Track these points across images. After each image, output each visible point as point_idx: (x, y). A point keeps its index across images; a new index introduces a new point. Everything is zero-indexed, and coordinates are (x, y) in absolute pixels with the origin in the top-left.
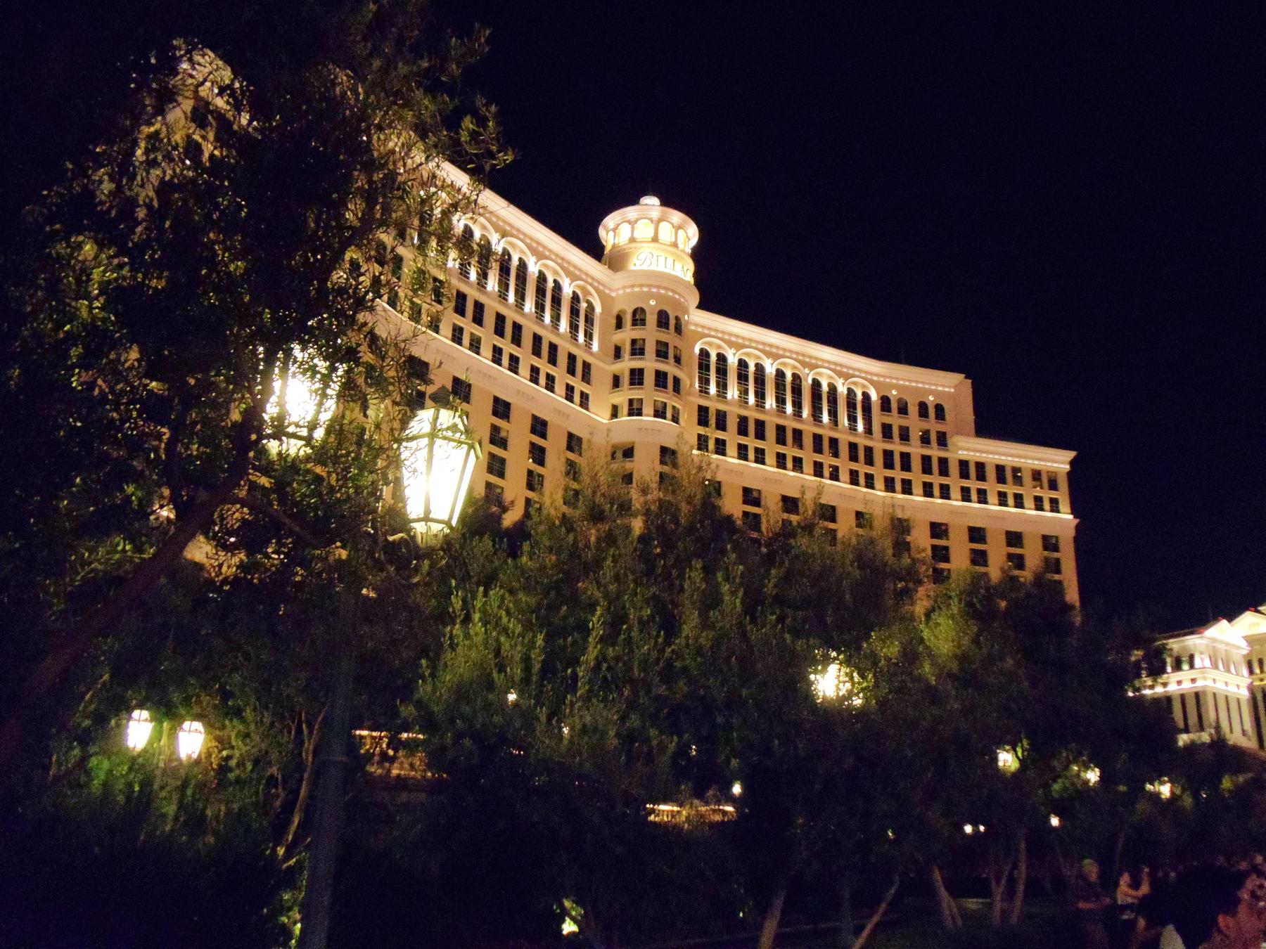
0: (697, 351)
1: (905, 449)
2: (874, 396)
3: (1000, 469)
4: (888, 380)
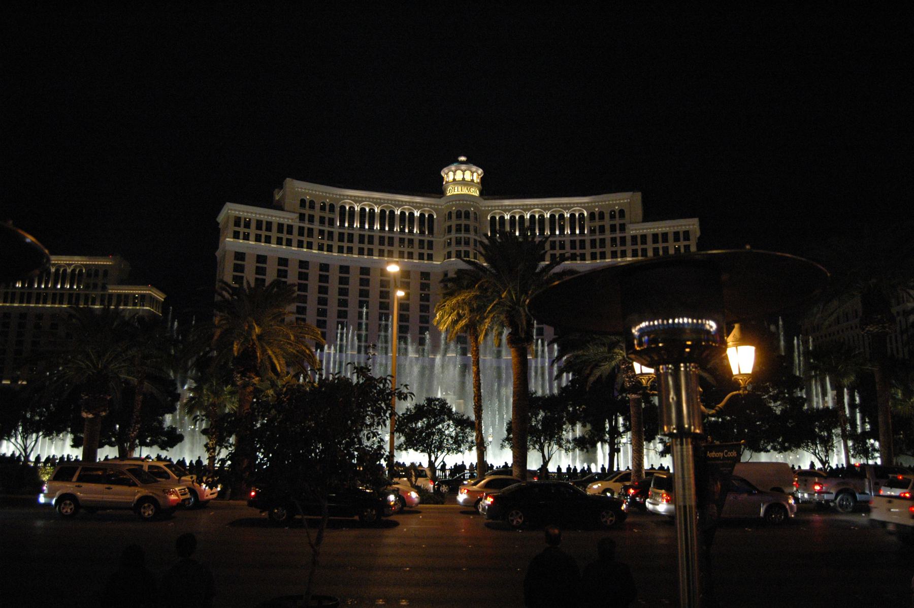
0: (489, 219)
1: (602, 237)
2: (586, 214)
3: (655, 236)
4: (593, 204)
